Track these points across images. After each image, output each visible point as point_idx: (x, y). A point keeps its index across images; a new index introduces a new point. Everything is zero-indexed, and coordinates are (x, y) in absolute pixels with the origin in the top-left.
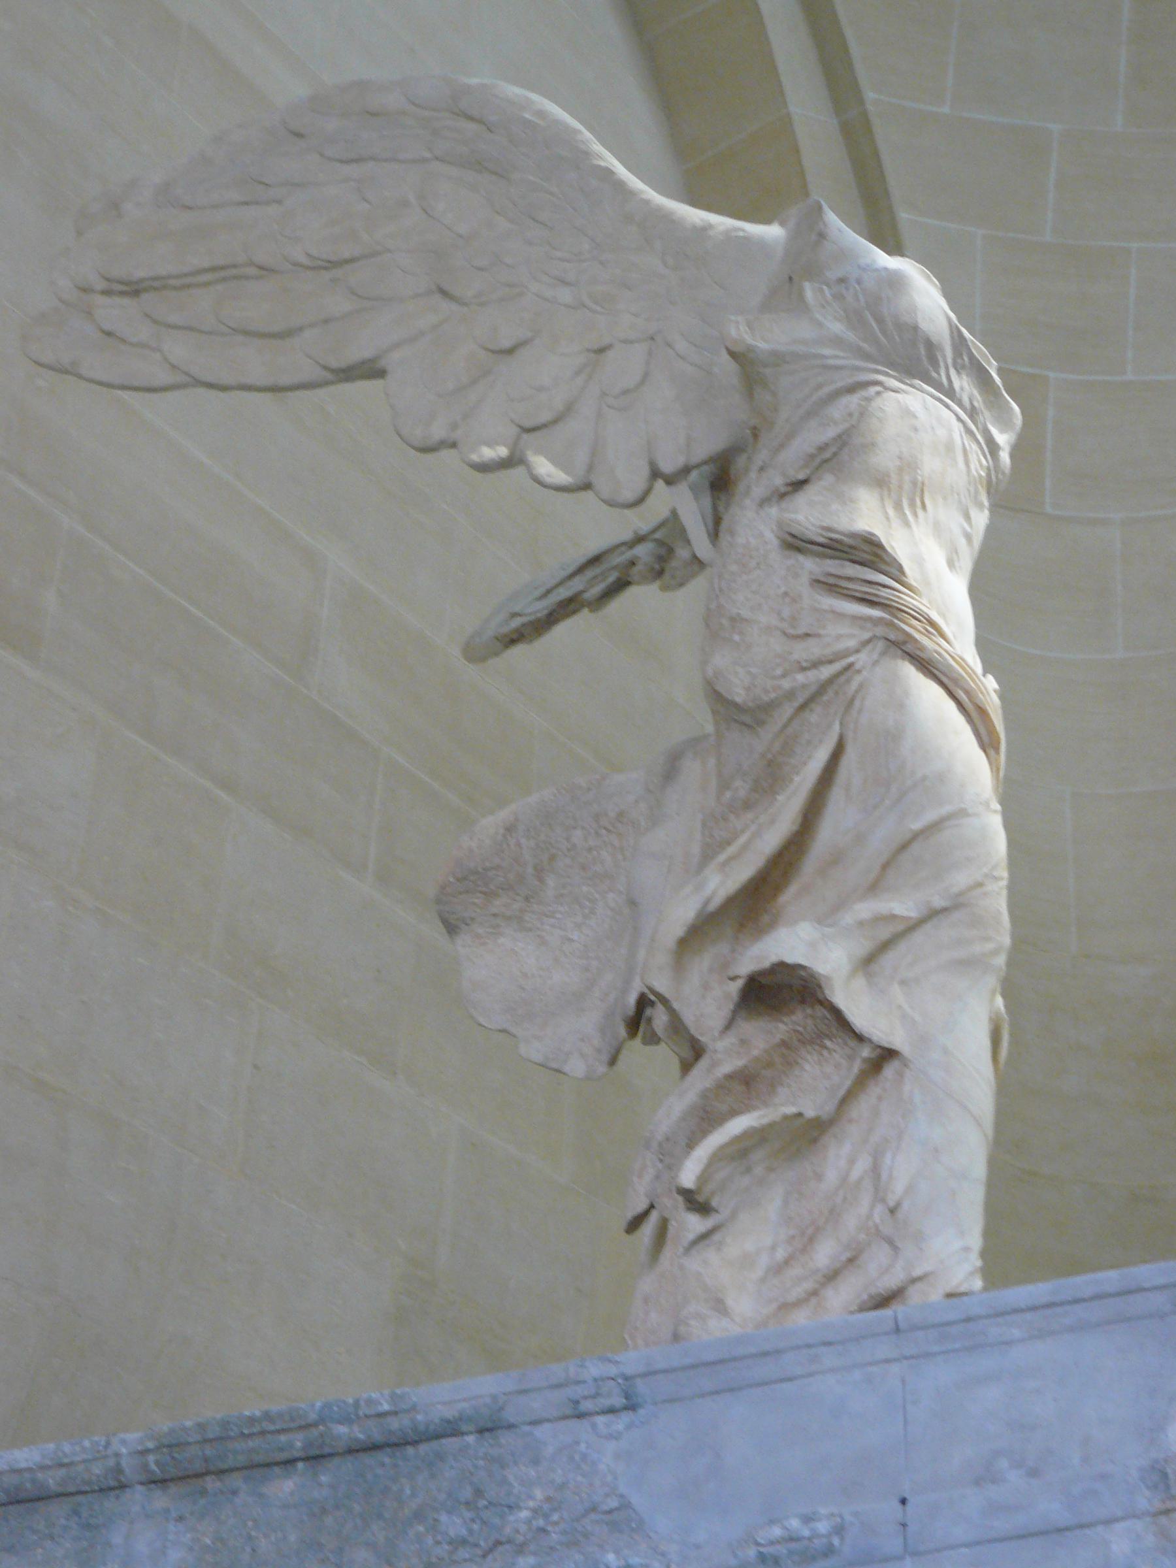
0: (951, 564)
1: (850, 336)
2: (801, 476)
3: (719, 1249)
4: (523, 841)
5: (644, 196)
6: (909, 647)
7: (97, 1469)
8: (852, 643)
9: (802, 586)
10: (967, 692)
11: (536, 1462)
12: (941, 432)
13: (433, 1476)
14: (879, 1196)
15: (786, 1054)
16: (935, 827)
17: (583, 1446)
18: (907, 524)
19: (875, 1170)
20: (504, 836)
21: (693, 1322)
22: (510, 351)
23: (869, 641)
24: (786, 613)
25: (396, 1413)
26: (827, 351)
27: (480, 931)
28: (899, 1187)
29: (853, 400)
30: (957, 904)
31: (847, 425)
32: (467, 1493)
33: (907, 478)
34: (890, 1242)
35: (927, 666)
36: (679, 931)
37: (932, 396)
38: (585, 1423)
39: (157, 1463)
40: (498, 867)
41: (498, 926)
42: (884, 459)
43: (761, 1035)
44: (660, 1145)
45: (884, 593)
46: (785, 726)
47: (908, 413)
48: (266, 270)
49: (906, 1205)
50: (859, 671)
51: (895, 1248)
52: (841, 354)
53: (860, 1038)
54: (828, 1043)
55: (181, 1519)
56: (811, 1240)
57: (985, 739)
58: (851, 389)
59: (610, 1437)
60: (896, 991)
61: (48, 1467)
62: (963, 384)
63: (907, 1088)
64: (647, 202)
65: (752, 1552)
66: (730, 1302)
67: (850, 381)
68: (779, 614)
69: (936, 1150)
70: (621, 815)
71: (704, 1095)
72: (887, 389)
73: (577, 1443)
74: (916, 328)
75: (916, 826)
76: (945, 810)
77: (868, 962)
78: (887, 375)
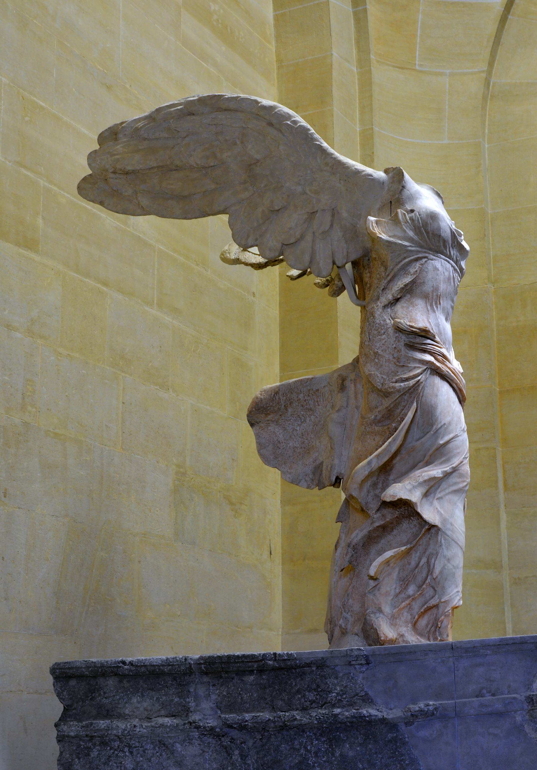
0: (446, 319)
1: (416, 238)
2: (399, 297)
3: (379, 590)
4: (281, 397)
5: (333, 156)
6: (438, 371)
7: (183, 668)
8: (419, 371)
9: (401, 345)
10: (456, 384)
11: (337, 678)
12: (447, 274)
13: (302, 679)
14: (430, 571)
15: (398, 521)
16: (448, 442)
17: (352, 674)
18: (434, 311)
19: (428, 562)
20: (274, 395)
21: (372, 615)
22: (278, 211)
23: (426, 369)
24: (395, 355)
25: (289, 660)
26: (407, 244)
27: (262, 425)
28: (437, 571)
29: (418, 265)
30: (455, 470)
31: (415, 276)
32: (314, 686)
33: (435, 294)
34: (434, 588)
35: (444, 377)
36: (361, 477)
37: (444, 259)
38: (352, 667)
39: (205, 667)
40: (271, 406)
41: (269, 423)
42: (428, 288)
43: (389, 515)
44: (354, 546)
45: (429, 347)
46: (396, 400)
47: (436, 269)
48: (177, 169)
49: (439, 577)
50: (422, 382)
51: (435, 591)
52: (413, 245)
53: (425, 521)
54: (412, 518)
55: (214, 685)
56: (407, 585)
57: (461, 399)
58: (417, 260)
59: (361, 672)
60: (436, 503)
61: (165, 666)
62: (454, 252)
63: (439, 538)
64: (335, 158)
65: (409, 714)
66: (383, 608)
67: (416, 256)
68: (393, 355)
69: (449, 559)
70: (318, 390)
71: (369, 532)
72: (429, 259)
73: (350, 673)
74: (440, 236)
75: (442, 442)
76: (451, 436)
77: (426, 495)
78: (429, 253)
